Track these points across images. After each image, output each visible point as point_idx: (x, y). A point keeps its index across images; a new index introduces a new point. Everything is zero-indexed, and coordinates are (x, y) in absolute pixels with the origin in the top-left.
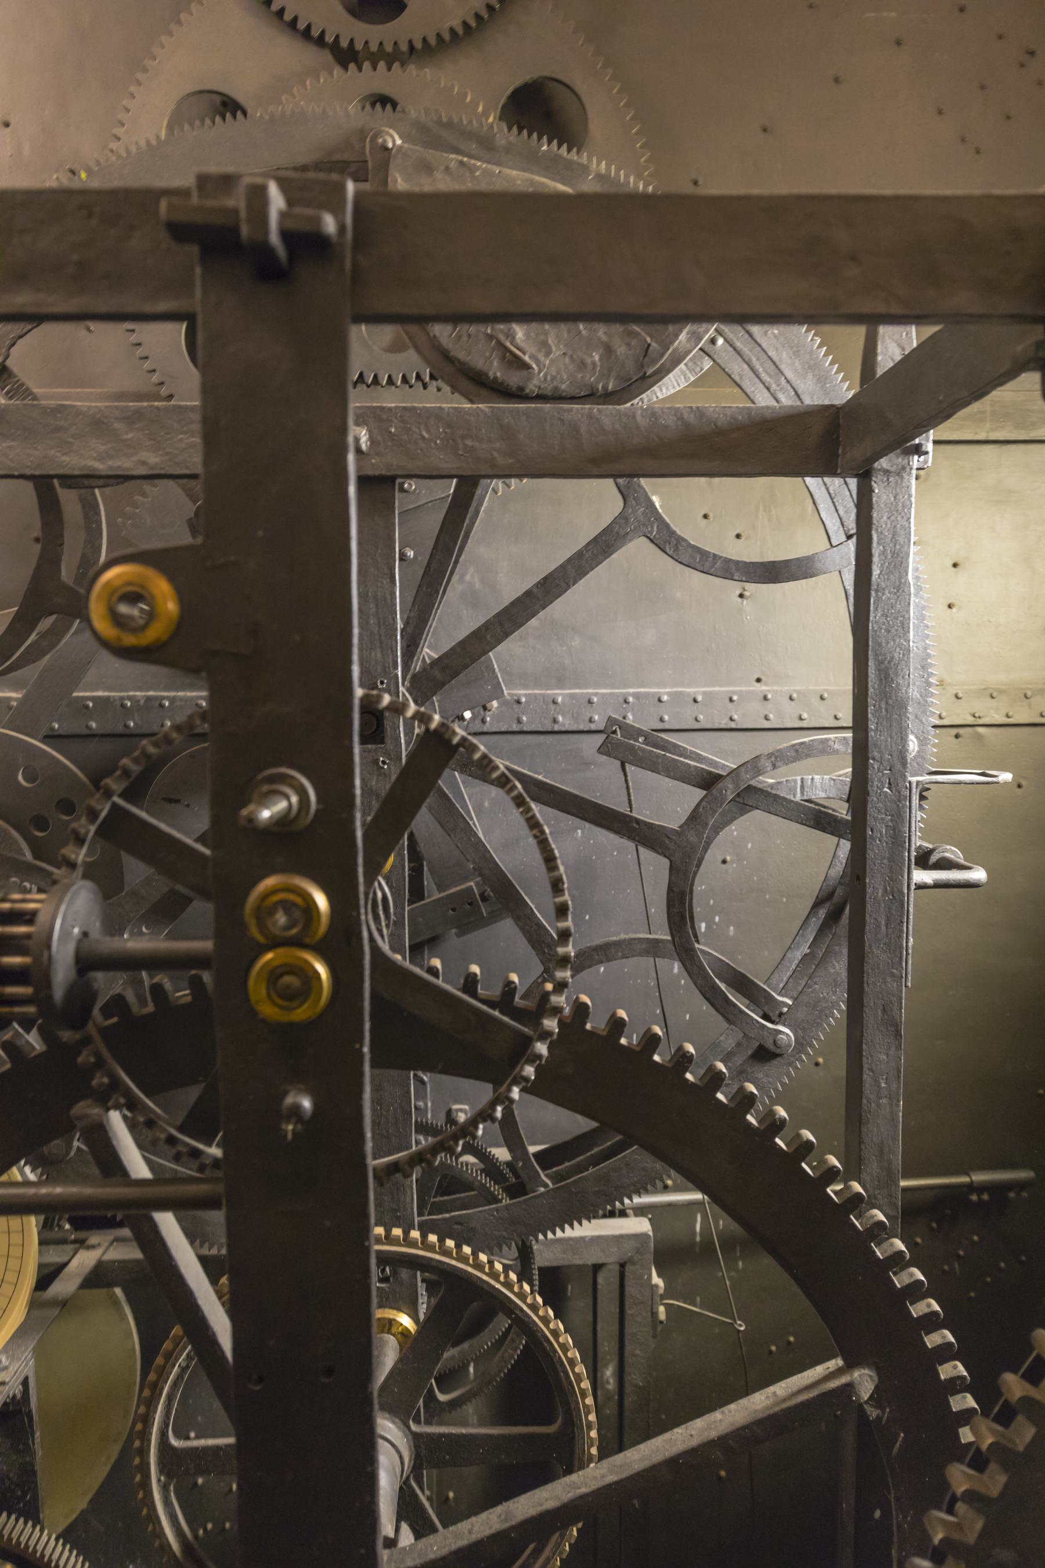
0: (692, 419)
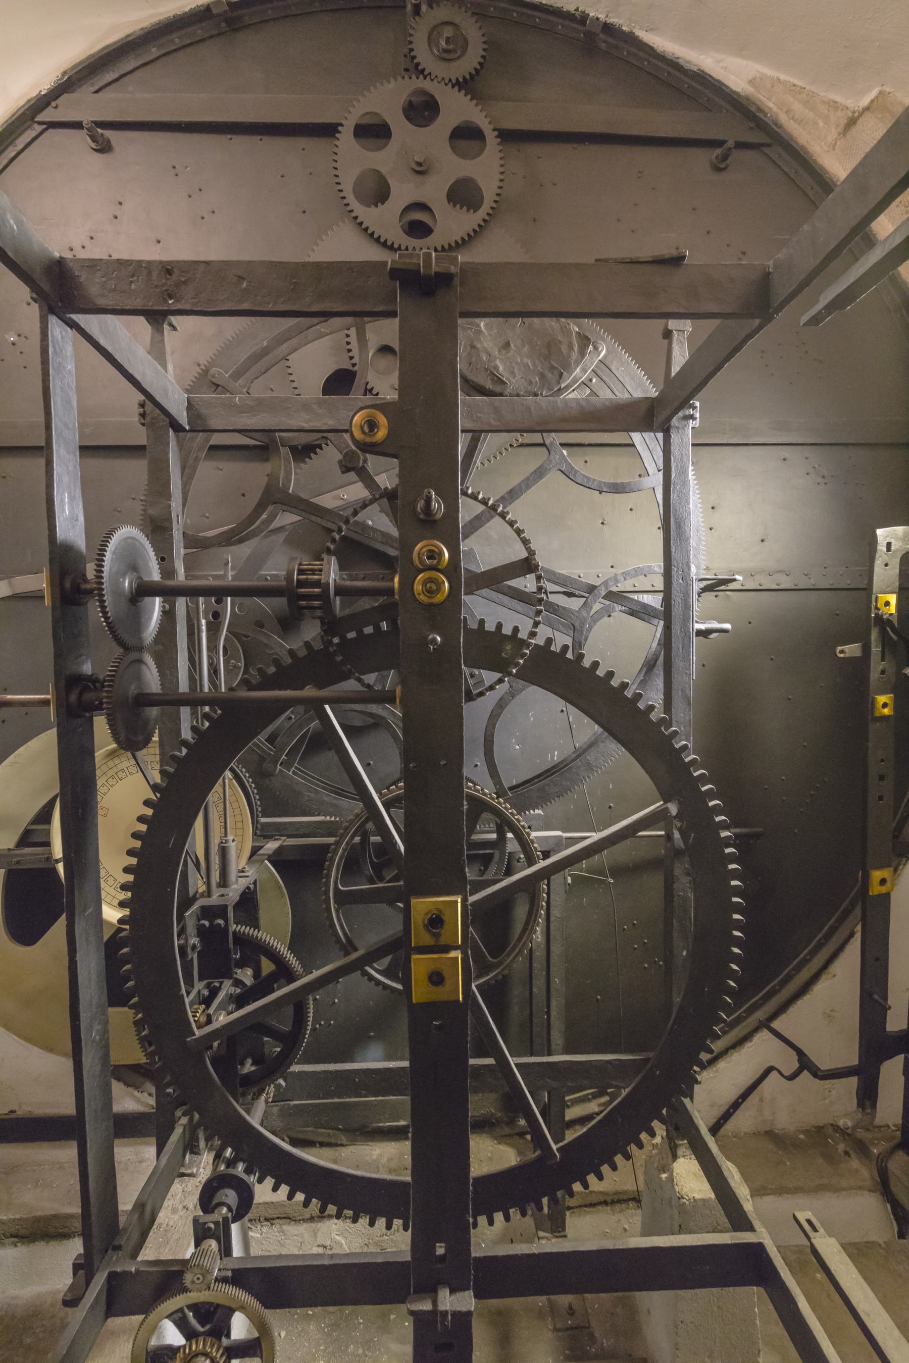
0: (584, 403)
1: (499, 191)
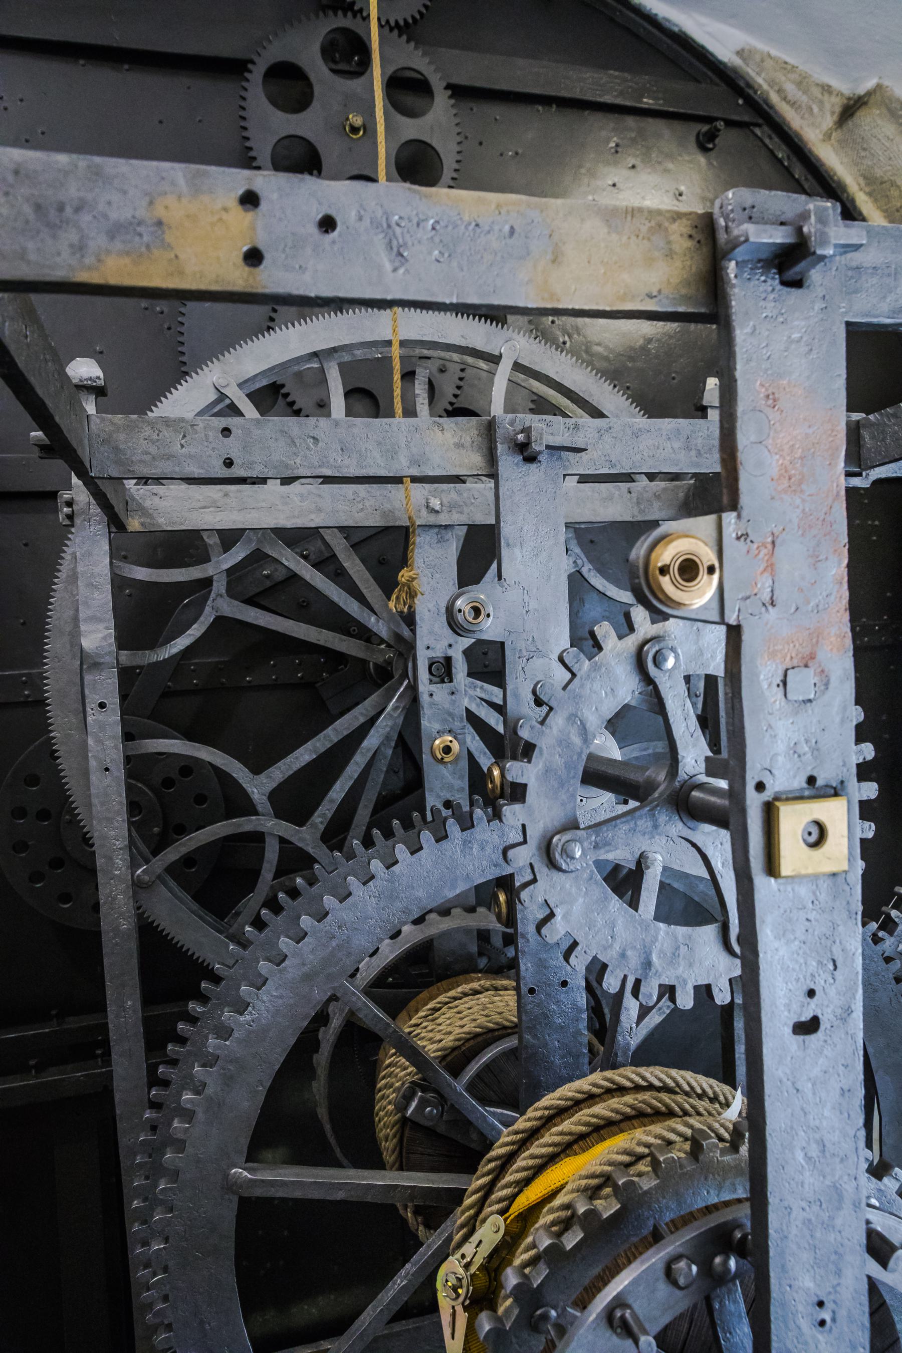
1: (457, 166)
